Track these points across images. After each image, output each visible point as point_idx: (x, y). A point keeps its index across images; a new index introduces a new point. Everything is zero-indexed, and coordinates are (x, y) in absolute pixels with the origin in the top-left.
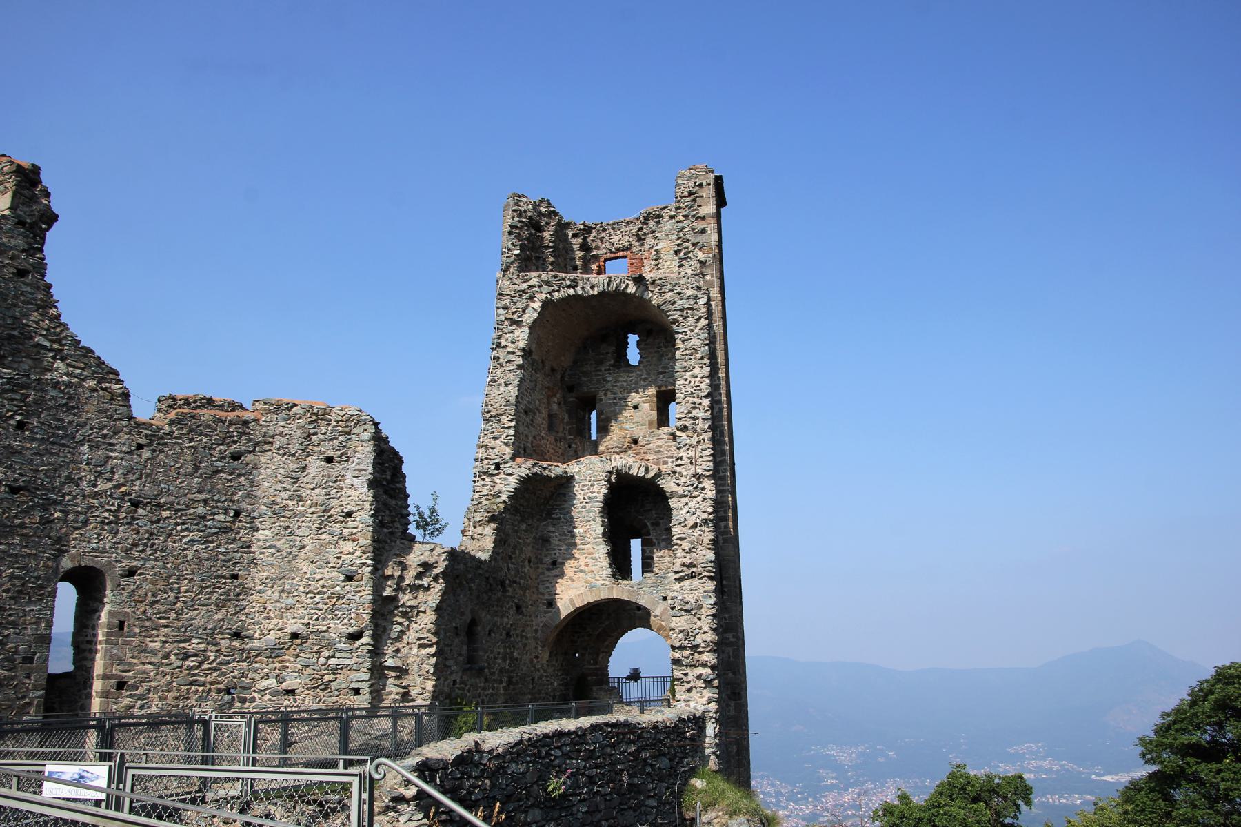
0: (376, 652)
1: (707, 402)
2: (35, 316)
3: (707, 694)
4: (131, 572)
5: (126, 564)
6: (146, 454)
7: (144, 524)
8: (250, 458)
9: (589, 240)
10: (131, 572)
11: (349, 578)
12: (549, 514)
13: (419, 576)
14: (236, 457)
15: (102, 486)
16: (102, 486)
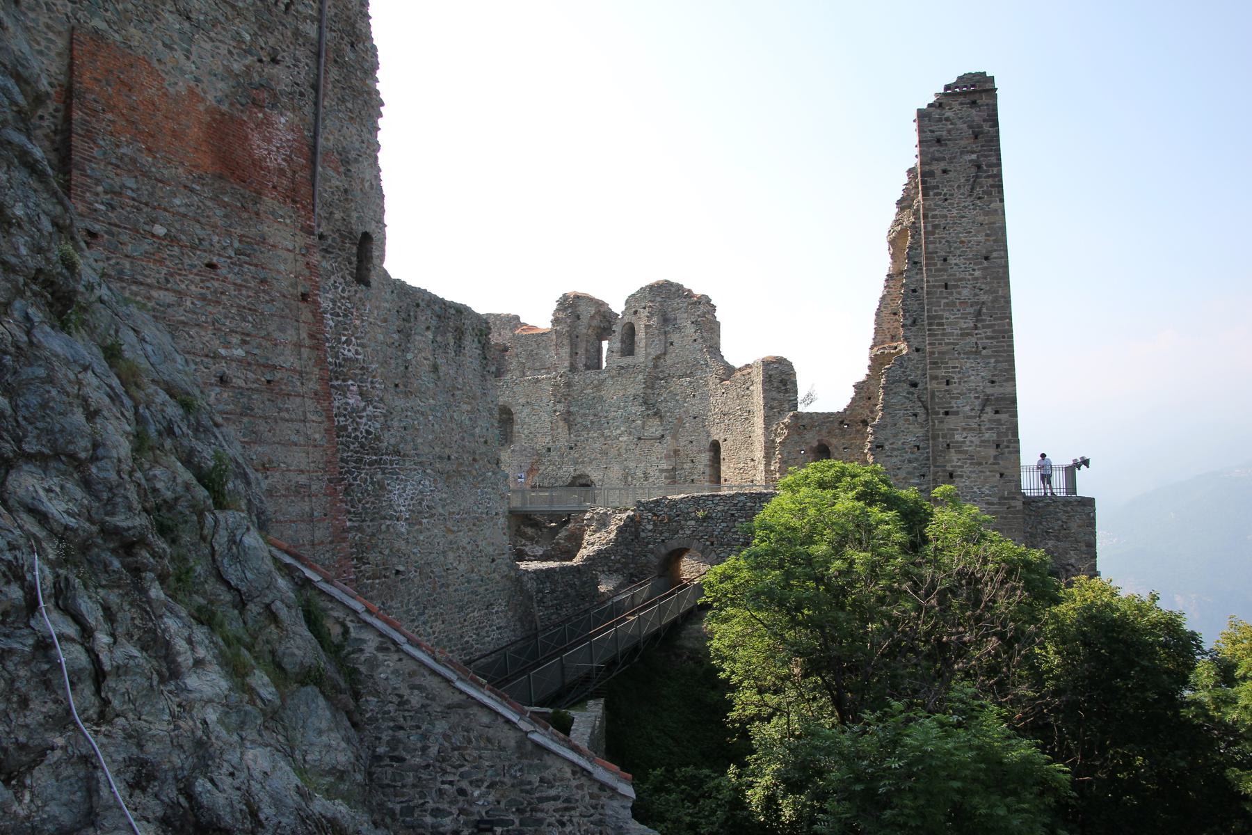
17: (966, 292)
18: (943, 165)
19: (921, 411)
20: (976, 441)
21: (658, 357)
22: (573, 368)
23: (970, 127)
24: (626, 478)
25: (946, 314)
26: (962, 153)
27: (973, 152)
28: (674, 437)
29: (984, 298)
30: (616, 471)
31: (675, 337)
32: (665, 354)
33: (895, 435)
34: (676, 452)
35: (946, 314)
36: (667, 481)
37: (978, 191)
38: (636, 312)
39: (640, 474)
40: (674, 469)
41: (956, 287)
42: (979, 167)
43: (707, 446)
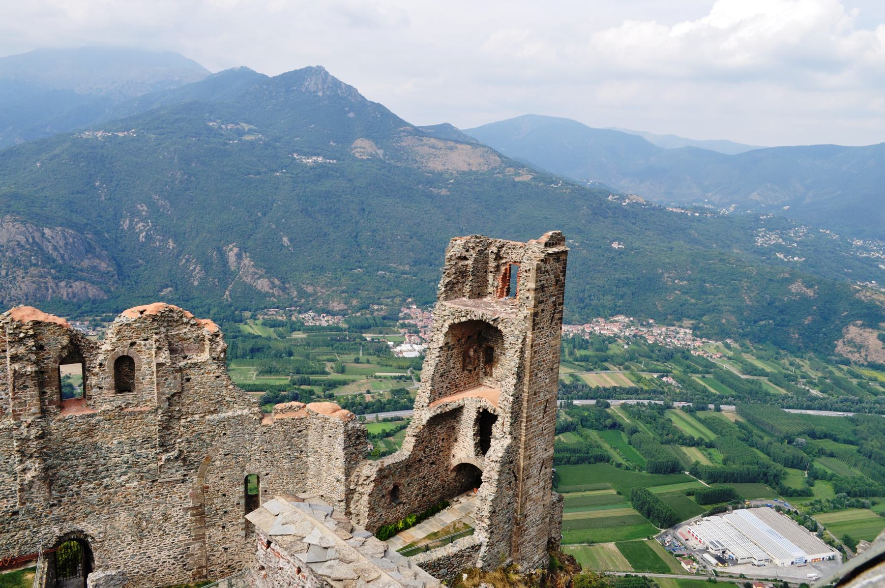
0: (348, 506)
1: (511, 399)
2: (224, 391)
3: (486, 534)
4: (267, 474)
5: (265, 472)
6: (267, 435)
7: (269, 459)
8: (304, 432)
9: (501, 253)
10: (267, 474)
11: (338, 481)
12: (455, 418)
13: (365, 480)
14: (300, 431)
15: (254, 448)
16: (254, 448)
17: (542, 394)
18: (542, 305)
19: (513, 479)
20: (536, 490)
21: (173, 395)
22: (44, 413)
23: (555, 277)
24: (139, 525)
25: (533, 413)
26: (550, 296)
27: (554, 295)
28: (202, 476)
29: (548, 397)
30: (123, 519)
31: (193, 374)
32: (182, 391)
33: (501, 501)
34: (205, 489)
35: (533, 413)
36: (194, 518)
37: (554, 323)
38: (133, 344)
39: (157, 516)
40: (202, 506)
41: (539, 392)
42: (555, 305)
43: (242, 481)
